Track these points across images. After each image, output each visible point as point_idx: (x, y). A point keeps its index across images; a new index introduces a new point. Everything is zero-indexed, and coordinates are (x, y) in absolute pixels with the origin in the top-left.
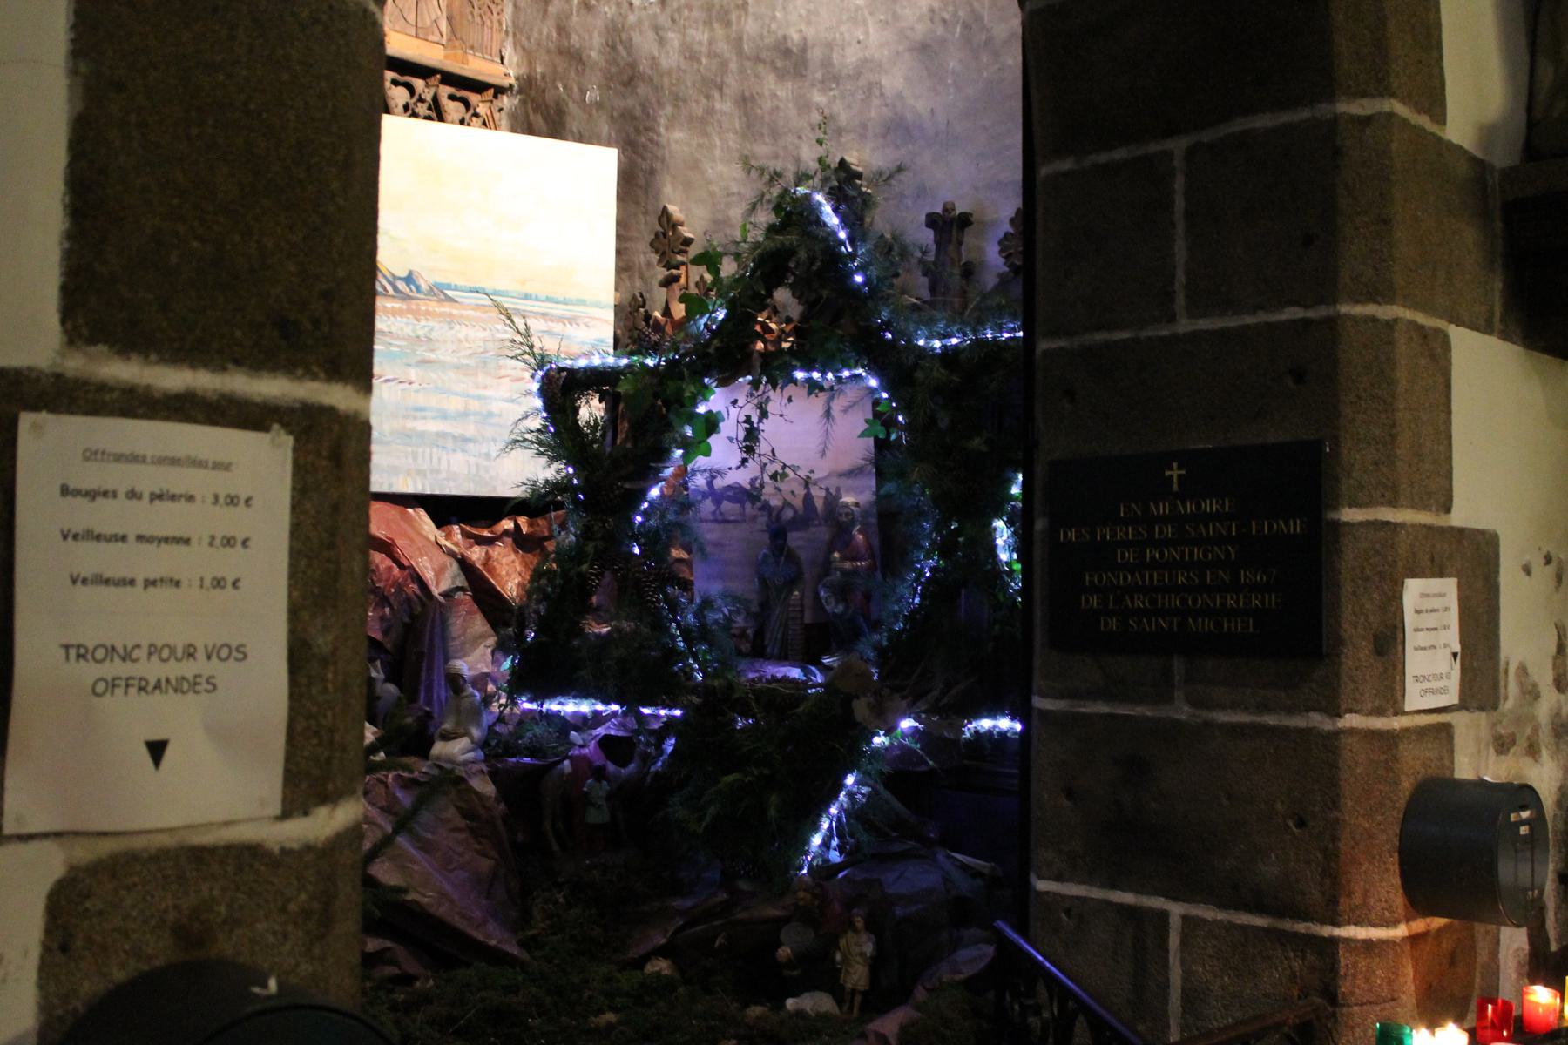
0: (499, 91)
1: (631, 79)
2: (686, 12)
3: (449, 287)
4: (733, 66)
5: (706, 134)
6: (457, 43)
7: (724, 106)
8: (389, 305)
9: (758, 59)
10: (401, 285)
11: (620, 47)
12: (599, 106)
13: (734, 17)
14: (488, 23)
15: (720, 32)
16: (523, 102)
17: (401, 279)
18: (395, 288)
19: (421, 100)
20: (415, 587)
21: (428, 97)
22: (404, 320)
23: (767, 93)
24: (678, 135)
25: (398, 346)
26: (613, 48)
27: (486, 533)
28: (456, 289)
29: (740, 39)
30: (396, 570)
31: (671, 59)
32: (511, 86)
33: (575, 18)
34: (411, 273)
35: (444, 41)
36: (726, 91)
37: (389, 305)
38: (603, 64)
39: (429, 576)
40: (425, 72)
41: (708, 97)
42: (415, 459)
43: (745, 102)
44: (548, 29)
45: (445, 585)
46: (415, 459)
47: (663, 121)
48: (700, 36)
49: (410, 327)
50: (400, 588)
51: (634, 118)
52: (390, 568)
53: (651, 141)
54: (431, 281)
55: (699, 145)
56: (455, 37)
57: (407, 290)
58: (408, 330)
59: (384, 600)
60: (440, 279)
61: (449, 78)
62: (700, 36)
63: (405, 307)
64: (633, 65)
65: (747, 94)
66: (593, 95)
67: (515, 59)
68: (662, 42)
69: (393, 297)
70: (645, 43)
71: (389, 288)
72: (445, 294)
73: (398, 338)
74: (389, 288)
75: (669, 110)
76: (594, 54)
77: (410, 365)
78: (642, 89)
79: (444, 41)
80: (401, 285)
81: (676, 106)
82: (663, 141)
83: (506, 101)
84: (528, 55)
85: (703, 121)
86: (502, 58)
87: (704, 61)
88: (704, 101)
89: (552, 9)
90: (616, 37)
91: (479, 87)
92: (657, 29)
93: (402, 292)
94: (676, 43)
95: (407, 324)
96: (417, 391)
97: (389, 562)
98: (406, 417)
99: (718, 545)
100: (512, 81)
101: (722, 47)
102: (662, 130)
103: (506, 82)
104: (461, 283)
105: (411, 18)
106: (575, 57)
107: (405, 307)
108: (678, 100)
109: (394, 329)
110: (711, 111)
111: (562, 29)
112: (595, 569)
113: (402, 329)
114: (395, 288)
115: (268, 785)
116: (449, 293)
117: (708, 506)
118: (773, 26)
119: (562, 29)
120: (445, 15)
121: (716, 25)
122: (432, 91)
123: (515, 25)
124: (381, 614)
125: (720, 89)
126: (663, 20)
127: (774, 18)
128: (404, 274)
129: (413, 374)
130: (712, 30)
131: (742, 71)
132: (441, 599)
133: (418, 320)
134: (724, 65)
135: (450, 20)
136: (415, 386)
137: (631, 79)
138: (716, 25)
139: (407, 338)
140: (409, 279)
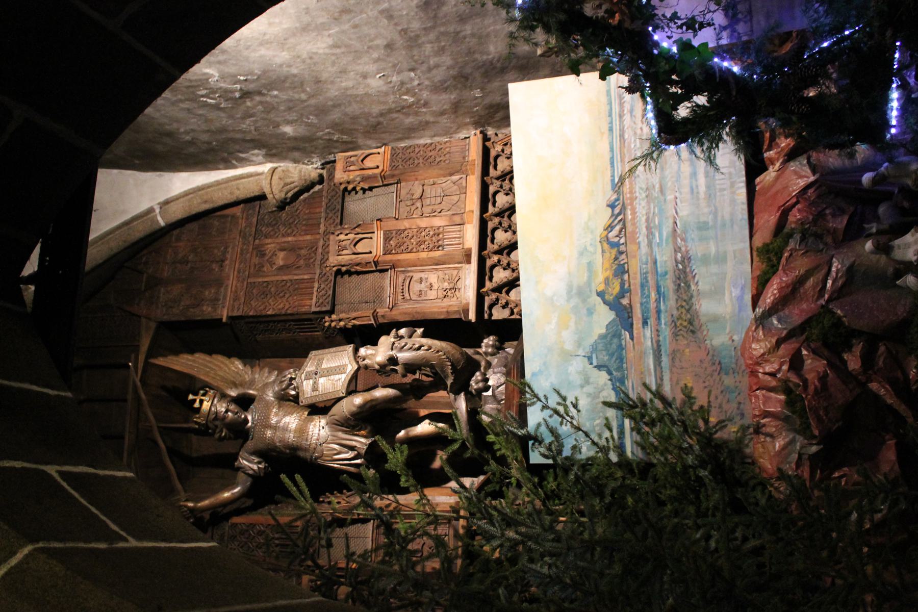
0: (486, 139)
1: (463, 77)
2: (416, 58)
3: (613, 180)
4: (442, 29)
5: (488, 35)
6: (464, 169)
7: (468, 29)
8: (630, 217)
9: (435, 16)
10: (617, 211)
11: (446, 85)
12: (482, 89)
13: (412, 34)
14: (447, 150)
15: (423, 39)
16: (489, 125)
17: (613, 211)
18: (619, 214)
19: (501, 187)
20: (810, 191)
21: (498, 183)
22: (637, 206)
23: (454, 9)
24: (492, 48)
25: (654, 208)
26: (446, 88)
27: (767, 135)
28: (613, 176)
29: (425, 29)
30: (799, 206)
31: (447, 60)
32: (481, 132)
33: (434, 108)
34: (608, 206)
35: (464, 176)
36: (458, 29)
37: (630, 217)
38: (458, 91)
39: (802, 183)
40: (484, 187)
41: (465, 38)
42: (724, 190)
43: (462, 19)
44: (444, 120)
45: (807, 170)
46: (724, 190)
47: (485, 57)
48: (428, 48)
49: (641, 202)
50: (812, 204)
51: (486, 72)
52: (799, 210)
53: (498, 61)
54: (611, 192)
55: (495, 37)
56: (460, 169)
57: (619, 206)
58: (643, 203)
59: (820, 216)
60: (609, 187)
61: (485, 172)
62: (428, 48)
63: (629, 207)
64: (455, 78)
65: (458, 19)
66: (478, 93)
67: (465, 132)
68: (437, 66)
69: (624, 215)
70: (439, 75)
71: (619, 218)
72: (618, 183)
73: (649, 209)
74: (619, 218)
75: (477, 56)
76: (453, 97)
77: (665, 200)
78: (468, 70)
79: (464, 176)
80: (617, 211)
81: (474, 52)
82: (497, 55)
83: (490, 132)
84: (460, 128)
85: (480, 37)
86: (466, 138)
87: (443, 44)
88: (467, 39)
89: (432, 119)
90: (439, 88)
91: (486, 152)
92: (430, 70)
93: (621, 210)
94: (436, 59)
95: (640, 204)
96: (681, 193)
97: (795, 210)
98: (698, 199)
99: (768, 16)
100: (478, 132)
101: (432, 36)
102: (490, 57)
103: (480, 136)
104: (609, 173)
105: (456, 198)
106: (456, 107)
107: (629, 207)
108: (470, 52)
109: (644, 212)
110: (473, 35)
111: (442, 113)
112: (795, 108)
113: (643, 207)
114: (619, 214)
116: (616, 180)
117: (741, 28)
118: (412, 14)
119: (442, 113)
120: (449, 178)
121: (420, 42)
122: (495, 181)
123: (445, 134)
124: (830, 217)
125: (458, 33)
126: (424, 67)
127: (407, 14)
128: (610, 210)
129: (670, 197)
130: (423, 43)
131: (443, 24)
132: (817, 176)
133: (636, 198)
134: (442, 34)
135: (451, 175)
136: (677, 195)
137: (463, 77)
138: (420, 42)
139: (648, 203)
140: (612, 206)
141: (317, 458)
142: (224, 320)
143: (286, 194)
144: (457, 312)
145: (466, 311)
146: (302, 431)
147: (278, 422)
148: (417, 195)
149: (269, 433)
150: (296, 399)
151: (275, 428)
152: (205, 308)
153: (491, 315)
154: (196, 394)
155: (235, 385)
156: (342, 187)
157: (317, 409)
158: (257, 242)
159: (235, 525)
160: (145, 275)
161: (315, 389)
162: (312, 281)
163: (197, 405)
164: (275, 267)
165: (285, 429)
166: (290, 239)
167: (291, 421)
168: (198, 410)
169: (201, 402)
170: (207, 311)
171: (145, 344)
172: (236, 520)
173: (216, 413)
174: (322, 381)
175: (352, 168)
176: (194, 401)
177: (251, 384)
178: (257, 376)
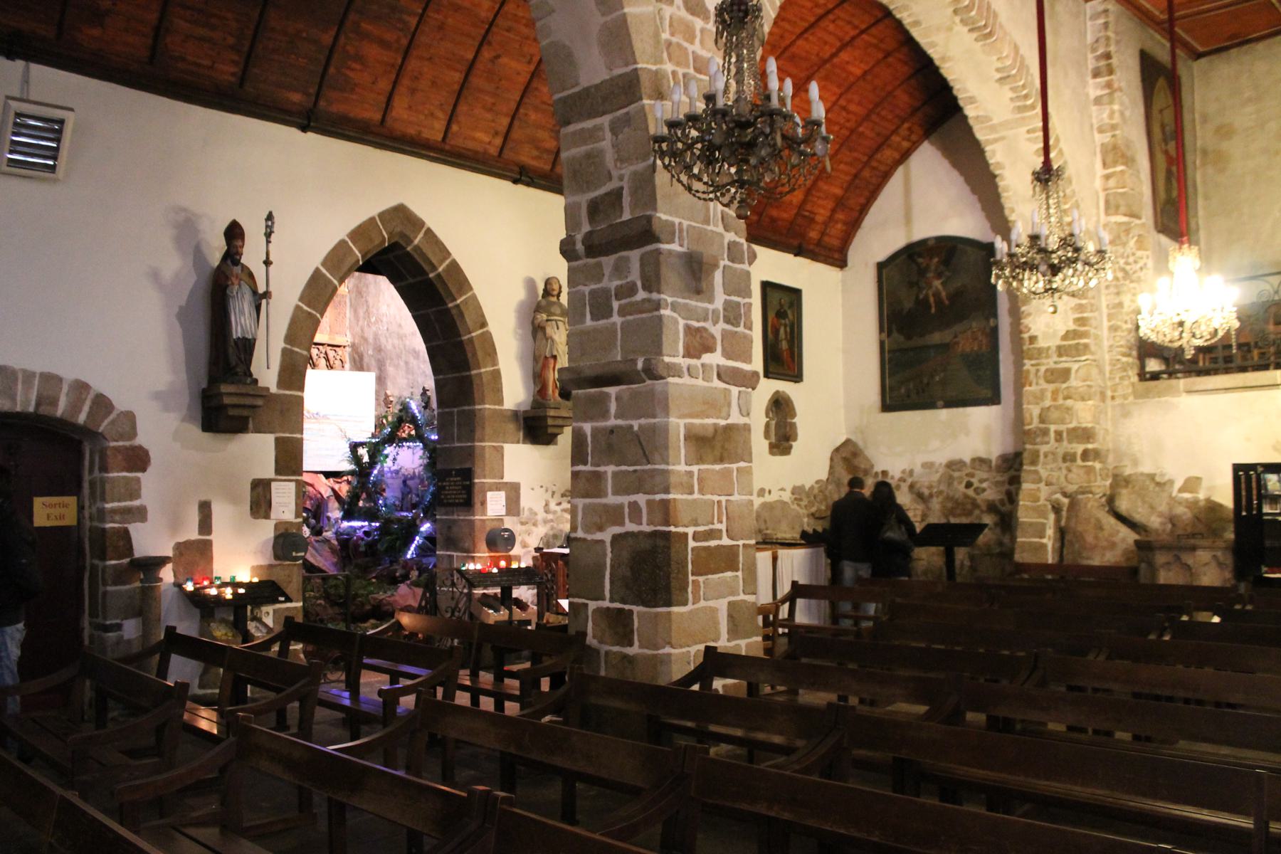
7: (402, 364)
12: (372, 356)
20: (319, 496)
21: (324, 352)
27: (339, 481)
31: (389, 347)
39: (323, 493)
43: (407, 363)
44: (358, 329)
45: (328, 495)
48: (396, 342)
50: (315, 496)
59: (311, 499)
62: (396, 342)
64: (380, 346)
66: (370, 352)
68: (387, 341)
70: (383, 340)
78: (382, 354)
84: (354, 336)
90: (376, 337)
92: (386, 337)
99: (392, 484)
101: (401, 346)
106: (365, 340)
108: (392, 359)
110: (399, 364)
111: (362, 330)
115: (293, 516)
117: (389, 475)
119: (362, 330)
126: (387, 335)
134: (401, 353)
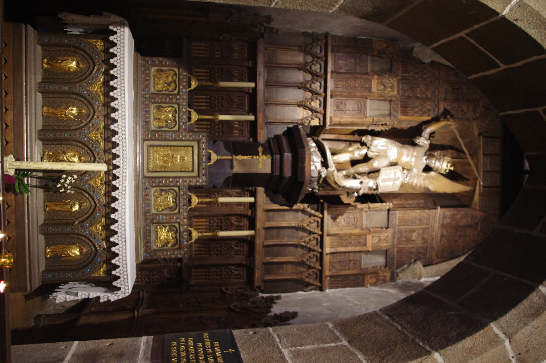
141: (393, 143)
142: (439, 208)
143: (413, 267)
144: (332, 207)
145: (328, 207)
146: (400, 155)
147: (411, 158)
148: (352, 262)
149: (415, 154)
150: (404, 169)
151: (413, 156)
152: (449, 214)
153: (318, 206)
154: (450, 170)
155: (432, 177)
156: (387, 268)
157: (393, 164)
158: (426, 245)
159: (429, 116)
160: (479, 229)
161: (395, 173)
162: (399, 226)
163: (449, 165)
164: (417, 232)
165: (408, 155)
166: (410, 246)
167: (405, 159)
168: (448, 162)
169: (447, 166)
170: (448, 212)
171: (476, 197)
172: (429, 118)
173: (440, 161)
174: (392, 176)
175: (382, 278)
176: (451, 166)
177: (425, 179)
178: (422, 182)
